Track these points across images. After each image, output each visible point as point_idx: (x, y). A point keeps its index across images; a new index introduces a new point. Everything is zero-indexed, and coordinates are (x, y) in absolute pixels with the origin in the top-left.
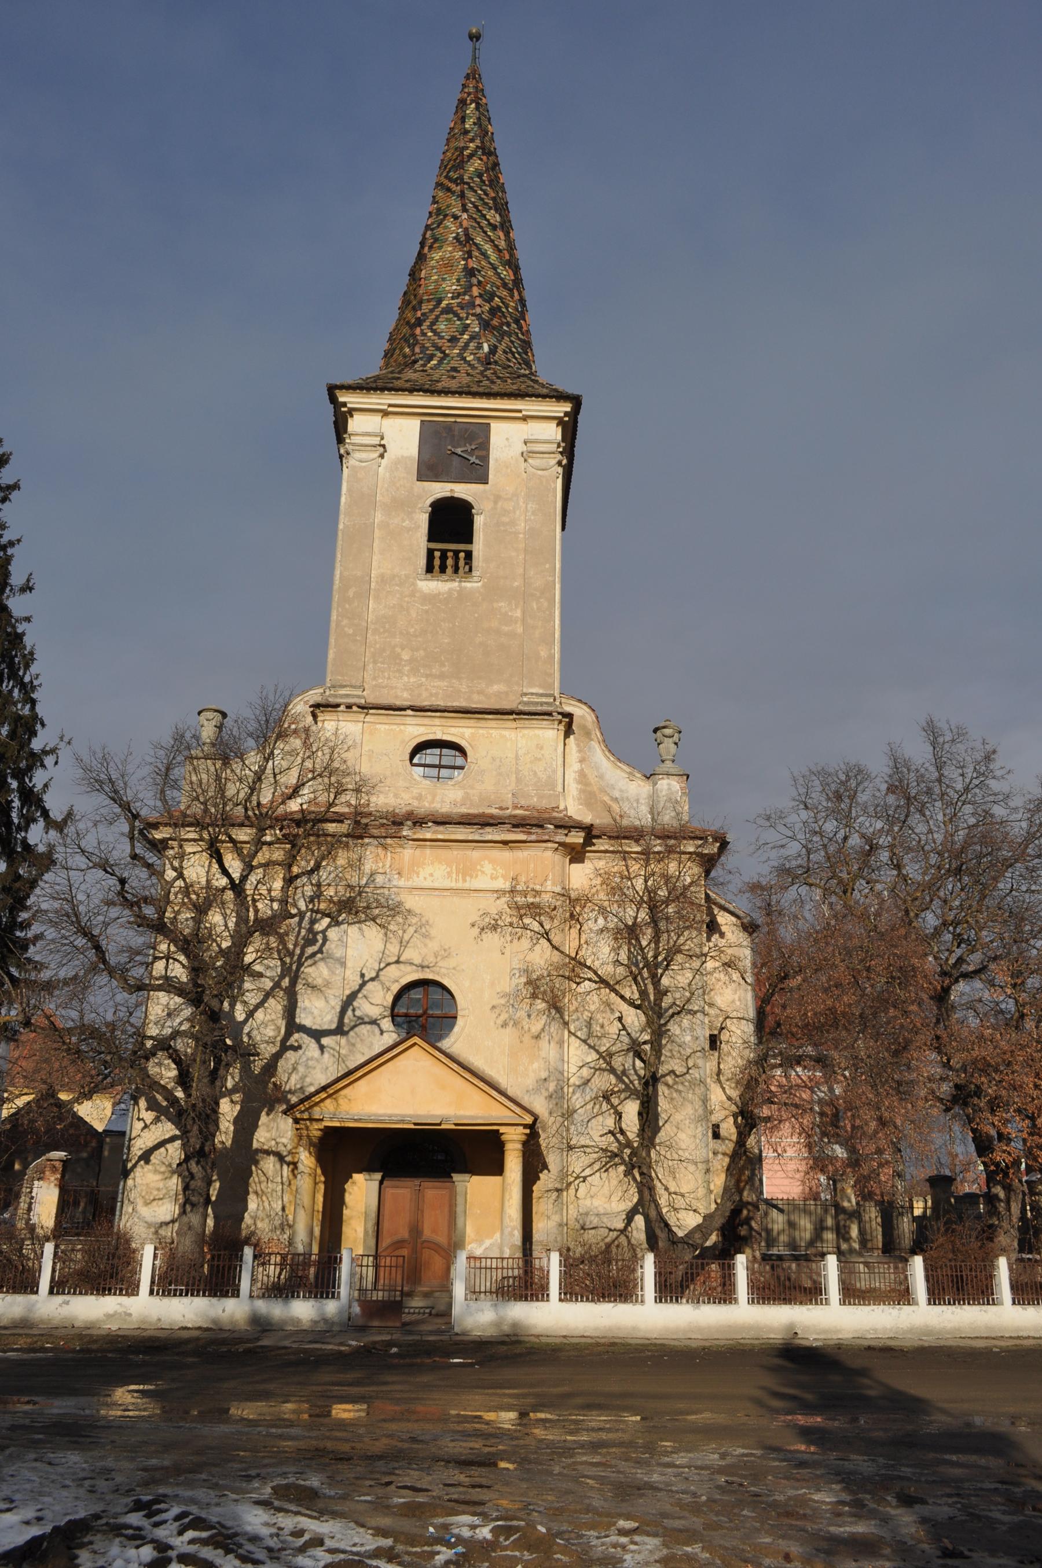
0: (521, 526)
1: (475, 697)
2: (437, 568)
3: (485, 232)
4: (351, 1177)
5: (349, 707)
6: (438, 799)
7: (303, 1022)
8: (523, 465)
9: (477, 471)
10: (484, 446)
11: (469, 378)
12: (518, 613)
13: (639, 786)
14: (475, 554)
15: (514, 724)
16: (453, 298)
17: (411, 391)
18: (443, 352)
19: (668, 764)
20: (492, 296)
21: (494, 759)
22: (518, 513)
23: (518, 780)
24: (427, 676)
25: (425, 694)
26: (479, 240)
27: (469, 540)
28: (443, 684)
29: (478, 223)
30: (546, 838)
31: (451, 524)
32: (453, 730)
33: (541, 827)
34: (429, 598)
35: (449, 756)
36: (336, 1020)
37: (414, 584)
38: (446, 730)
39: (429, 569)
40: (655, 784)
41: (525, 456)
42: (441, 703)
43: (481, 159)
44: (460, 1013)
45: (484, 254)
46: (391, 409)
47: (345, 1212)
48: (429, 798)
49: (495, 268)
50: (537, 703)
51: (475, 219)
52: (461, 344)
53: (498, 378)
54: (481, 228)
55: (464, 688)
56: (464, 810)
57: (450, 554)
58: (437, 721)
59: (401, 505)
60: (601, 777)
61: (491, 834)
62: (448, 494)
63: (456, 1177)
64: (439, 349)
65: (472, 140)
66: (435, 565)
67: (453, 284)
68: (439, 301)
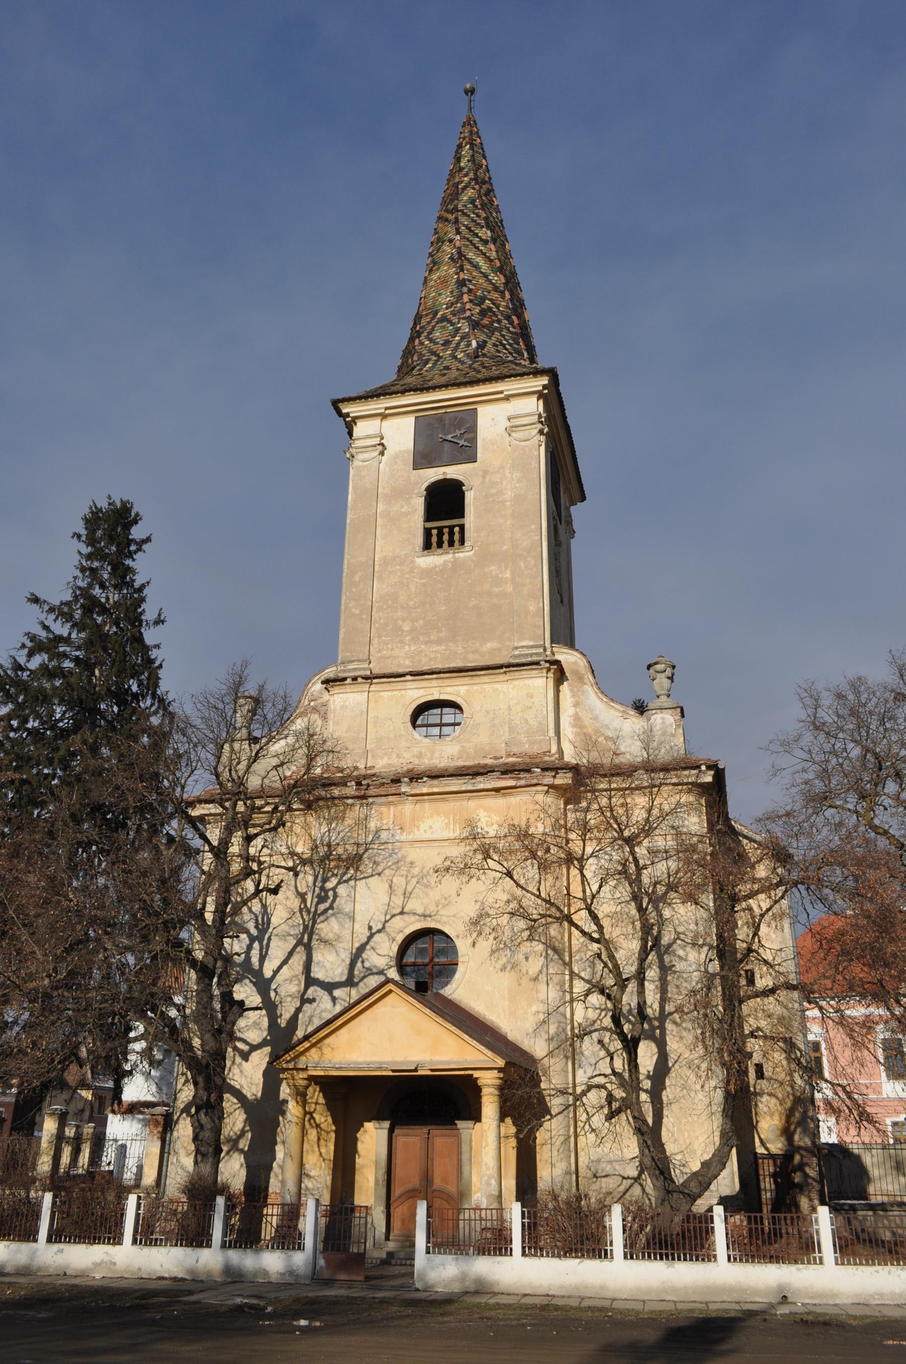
0: (509, 495)
1: (471, 656)
2: (434, 545)
3: (477, 248)
4: (363, 1126)
5: (355, 679)
6: (437, 755)
7: (316, 976)
8: (508, 439)
9: (466, 452)
11: (457, 373)
12: (508, 574)
13: (634, 723)
14: (467, 527)
15: (505, 677)
16: (447, 308)
17: (403, 392)
18: (438, 356)
19: (663, 698)
20: (483, 299)
21: (488, 712)
22: (504, 483)
23: (511, 730)
24: (426, 643)
25: (424, 660)
26: (471, 255)
27: (462, 515)
29: (471, 241)
30: (535, 781)
31: (445, 502)
32: (449, 689)
33: (528, 771)
34: (427, 573)
35: (449, 716)
36: (346, 972)
37: (413, 562)
38: (443, 690)
39: (427, 546)
40: (649, 719)
41: (510, 431)
42: (439, 666)
43: (474, 189)
44: (460, 959)
45: (476, 267)
46: (388, 412)
47: (357, 1160)
48: (429, 755)
49: (485, 276)
50: (527, 655)
51: (468, 239)
52: (453, 345)
53: (484, 367)
54: (474, 245)
55: (460, 650)
56: (461, 763)
57: (446, 530)
59: (399, 493)
60: (596, 718)
61: (482, 783)
62: (441, 477)
63: (460, 1124)
65: (466, 175)
67: (448, 296)
68: (436, 313)
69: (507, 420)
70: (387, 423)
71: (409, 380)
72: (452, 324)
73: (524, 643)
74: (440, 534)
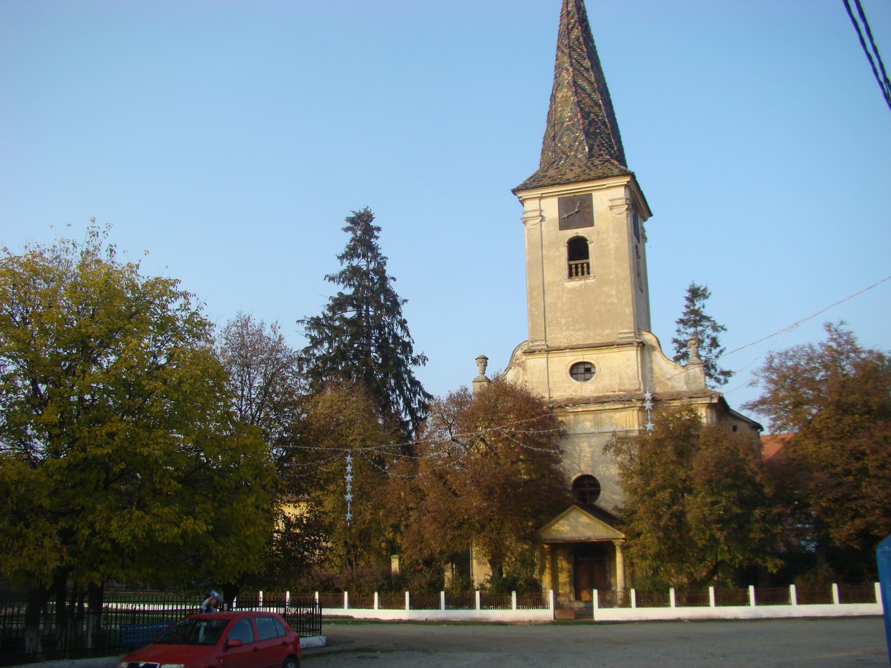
0: (612, 246)
1: (597, 338)
3: (583, 75)
8: (609, 213)
9: (588, 221)
10: (590, 206)
11: (579, 170)
12: (614, 292)
14: (591, 264)
15: (616, 350)
20: (590, 113)
23: (620, 377)
24: (574, 330)
25: (574, 340)
26: (580, 82)
27: (588, 258)
28: (581, 333)
31: (578, 250)
34: (571, 291)
39: (570, 275)
41: (611, 208)
45: (584, 90)
49: (589, 95)
54: (581, 73)
55: (591, 334)
58: (580, 353)
60: (661, 369)
61: (607, 406)
64: (564, 153)
65: (572, 18)
66: (573, 273)
69: (608, 199)
70: (543, 201)
71: (552, 172)
72: (573, 133)
73: (624, 331)
74: (577, 267)
